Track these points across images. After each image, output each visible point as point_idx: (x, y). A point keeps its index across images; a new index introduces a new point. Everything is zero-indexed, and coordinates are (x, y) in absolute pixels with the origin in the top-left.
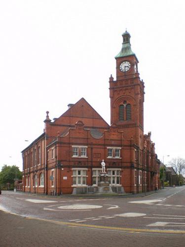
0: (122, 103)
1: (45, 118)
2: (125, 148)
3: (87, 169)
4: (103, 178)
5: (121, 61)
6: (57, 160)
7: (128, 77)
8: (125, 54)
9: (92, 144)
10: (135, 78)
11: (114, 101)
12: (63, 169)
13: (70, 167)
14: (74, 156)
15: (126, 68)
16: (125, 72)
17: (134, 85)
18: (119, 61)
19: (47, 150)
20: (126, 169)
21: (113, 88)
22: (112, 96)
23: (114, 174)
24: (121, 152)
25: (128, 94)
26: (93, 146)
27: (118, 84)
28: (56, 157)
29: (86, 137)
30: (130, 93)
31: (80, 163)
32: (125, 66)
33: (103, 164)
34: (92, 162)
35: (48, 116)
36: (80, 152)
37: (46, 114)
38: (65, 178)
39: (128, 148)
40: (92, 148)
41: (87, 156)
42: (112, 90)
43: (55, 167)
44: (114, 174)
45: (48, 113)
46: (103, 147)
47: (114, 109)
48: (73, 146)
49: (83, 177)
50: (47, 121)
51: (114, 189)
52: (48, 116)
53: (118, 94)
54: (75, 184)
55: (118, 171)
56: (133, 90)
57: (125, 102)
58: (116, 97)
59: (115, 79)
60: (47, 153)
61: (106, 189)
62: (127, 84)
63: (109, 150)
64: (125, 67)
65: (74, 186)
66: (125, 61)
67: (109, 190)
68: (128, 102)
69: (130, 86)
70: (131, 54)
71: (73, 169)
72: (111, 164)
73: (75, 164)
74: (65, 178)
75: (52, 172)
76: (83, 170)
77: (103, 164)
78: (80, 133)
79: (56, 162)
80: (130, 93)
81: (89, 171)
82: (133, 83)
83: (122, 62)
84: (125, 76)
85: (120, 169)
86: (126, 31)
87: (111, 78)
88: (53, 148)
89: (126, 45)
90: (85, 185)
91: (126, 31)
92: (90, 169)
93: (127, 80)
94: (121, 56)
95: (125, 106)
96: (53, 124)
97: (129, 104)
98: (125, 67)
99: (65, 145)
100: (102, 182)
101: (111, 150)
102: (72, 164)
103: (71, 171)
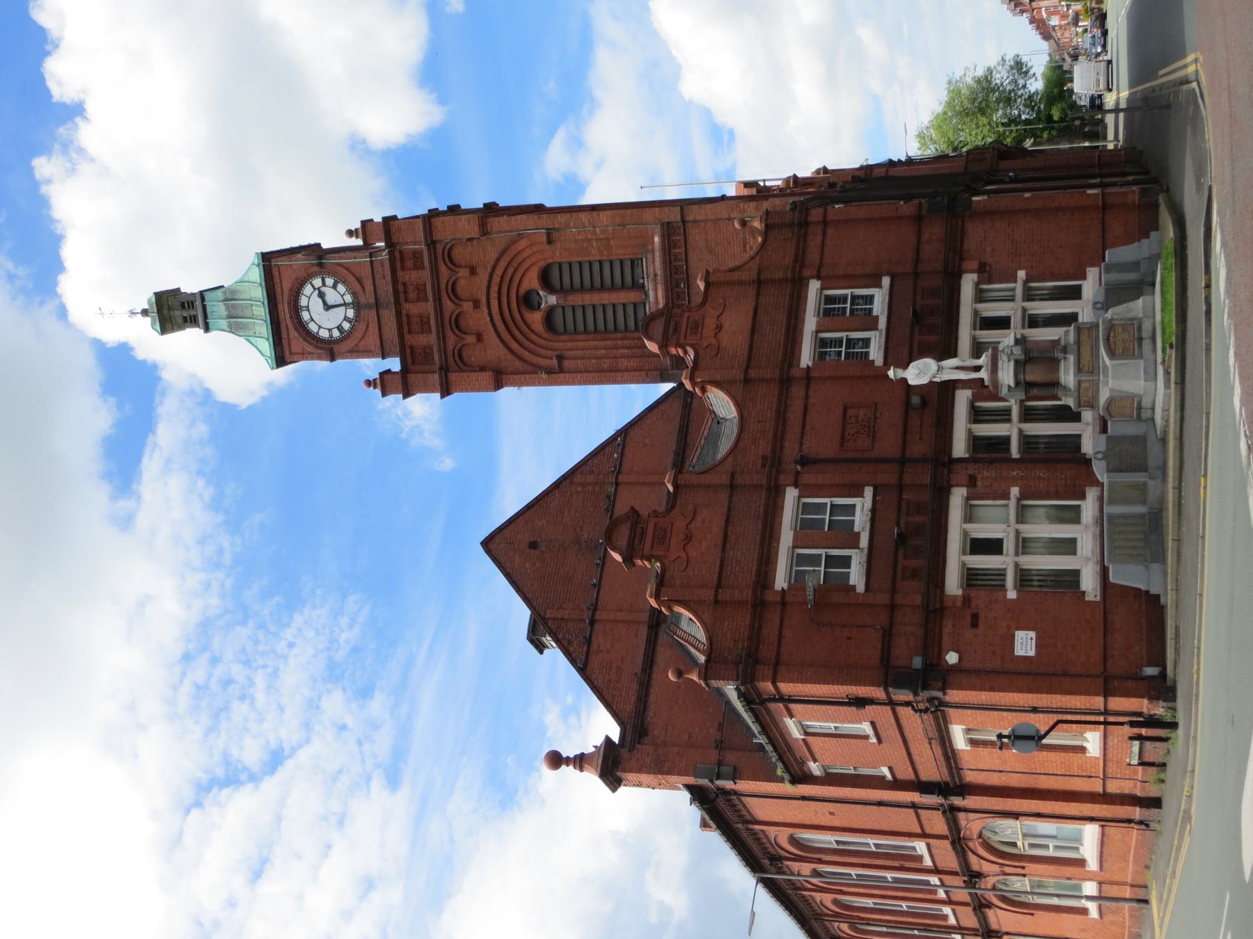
0: (536, 318)
1: (591, 780)
2: (813, 255)
3: (958, 497)
4: (1034, 375)
5: (293, 333)
6: (878, 693)
7: (386, 289)
8: (261, 311)
9: (774, 462)
10: (390, 244)
11: (518, 364)
12: (952, 658)
13: (935, 607)
14: (856, 576)
15: (332, 297)
16: (356, 305)
17: (432, 244)
18: (297, 343)
19: (807, 778)
20: (971, 244)
21: (445, 370)
22: (487, 376)
23: (1002, 323)
24: (850, 280)
26: (791, 449)
27: (420, 340)
28: (860, 702)
29: (723, 497)
30: (473, 271)
31: (912, 540)
32: (326, 308)
33: (920, 372)
34: (903, 461)
35: (580, 761)
36: (822, 537)
37: (568, 771)
38: (1025, 644)
39: (814, 243)
40: (804, 461)
41: (860, 494)
42: (453, 377)
43: (938, 713)
44: (1002, 323)
46: (797, 392)
47: (567, 364)
48: (781, 582)
49: (1020, 519)
50: (612, 765)
51: (1115, 294)
52: (580, 761)
53: (479, 338)
54: (1076, 574)
55: (980, 297)
56: (458, 254)
57: (528, 301)
58: (494, 350)
59: (394, 364)
60: (831, 779)
61: (1127, 342)
62: (421, 289)
63: (820, 357)
64: (328, 307)
65: (1089, 584)
66: (296, 309)
67: (1134, 325)
68: (532, 281)
69: (435, 273)
70: (256, 275)
71: (953, 584)
72: (928, 328)
73: (914, 574)
74: (1025, 644)
75: (973, 742)
76: (969, 517)
77: (920, 372)
78: (688, 538)
79: (892, 703)
81: (972, 482)
82: (417, 255)
83: (302, 327)
84: (377, 305)
85: (968, 283)
86: (145, 312)
87: (384, 383)
88: (793, 729)
89: (217, 308)
90: (1088, 508)
91: (145, 312)
92: (961, 473)
93: (400, 293)
94: (264, 328)
95: (553, 300)
96: (636, 725)
98: (328, 307)
99: (770, 630)
100: (1068, 376)
101: (823, 343)
102: (912, 594)
103: (966, 600)
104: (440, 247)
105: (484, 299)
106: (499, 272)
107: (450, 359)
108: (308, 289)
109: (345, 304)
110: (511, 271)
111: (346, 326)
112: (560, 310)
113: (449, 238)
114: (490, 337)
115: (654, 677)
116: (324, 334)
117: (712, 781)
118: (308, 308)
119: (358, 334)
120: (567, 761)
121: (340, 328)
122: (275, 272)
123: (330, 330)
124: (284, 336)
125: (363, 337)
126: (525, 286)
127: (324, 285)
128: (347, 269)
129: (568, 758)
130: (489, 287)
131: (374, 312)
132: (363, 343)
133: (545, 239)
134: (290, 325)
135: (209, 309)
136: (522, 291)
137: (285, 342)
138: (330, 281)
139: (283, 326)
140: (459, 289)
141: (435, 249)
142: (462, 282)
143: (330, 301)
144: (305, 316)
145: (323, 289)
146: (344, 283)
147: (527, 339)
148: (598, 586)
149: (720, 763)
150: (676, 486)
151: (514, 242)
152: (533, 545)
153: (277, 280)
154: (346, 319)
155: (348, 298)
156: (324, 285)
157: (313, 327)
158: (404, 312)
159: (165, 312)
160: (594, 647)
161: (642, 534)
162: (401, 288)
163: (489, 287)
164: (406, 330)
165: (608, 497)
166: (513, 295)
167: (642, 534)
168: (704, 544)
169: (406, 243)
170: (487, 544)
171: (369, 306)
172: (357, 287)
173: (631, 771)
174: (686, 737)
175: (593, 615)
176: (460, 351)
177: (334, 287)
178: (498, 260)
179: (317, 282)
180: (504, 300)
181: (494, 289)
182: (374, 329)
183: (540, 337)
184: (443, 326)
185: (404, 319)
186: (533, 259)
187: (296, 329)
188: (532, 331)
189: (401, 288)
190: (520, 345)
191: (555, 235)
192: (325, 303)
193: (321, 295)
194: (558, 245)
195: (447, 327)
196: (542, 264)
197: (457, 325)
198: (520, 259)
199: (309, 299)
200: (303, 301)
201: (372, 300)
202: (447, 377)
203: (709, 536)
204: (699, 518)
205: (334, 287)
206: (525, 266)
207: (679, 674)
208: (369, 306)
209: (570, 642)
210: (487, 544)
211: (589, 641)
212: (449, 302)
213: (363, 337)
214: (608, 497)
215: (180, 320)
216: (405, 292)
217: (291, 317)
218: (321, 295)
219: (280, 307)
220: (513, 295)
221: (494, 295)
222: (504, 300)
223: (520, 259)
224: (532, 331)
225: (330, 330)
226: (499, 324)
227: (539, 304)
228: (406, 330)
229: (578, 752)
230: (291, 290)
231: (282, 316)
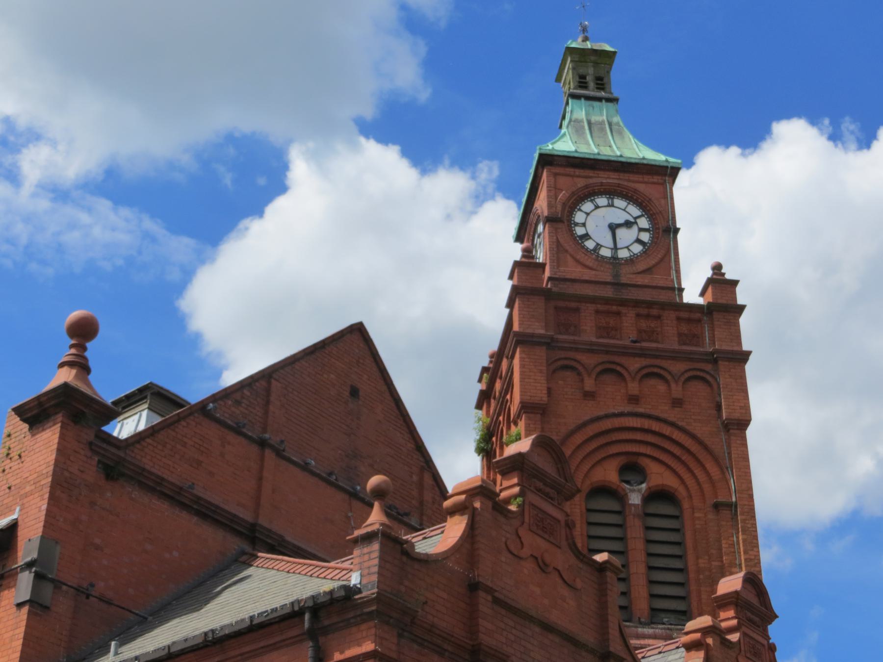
0: (609, 474)
5: (581, 183)
15: (626, 236)
21: (549, 344)
25: (664, 410)
30: (677, 403)
45: (84, 331)
53: (589, 395)
57: (632, 469)
64: (613, 228)
66: (612, 192)
68: (659, 476)
80: (677, 403)
82: (695, 338)
83: (589, 194)
84: (617, 285)
95: (635, 499)
97: (658, 495)
98: (613, 228)
104: (709, 367)
105: (641, 410)
106: (677, 435)
107: (562, 354)
108: (635, 211)
109: (615, 248)
110: (677, 451)
111: (590, 244)
112: (616, 507)
113: (722, 381)
114: (589, 410)
115: (184, 515)
116: (579, 217)
117: (29, 565)
118: (611, 205)
119: (580, 256)
120: (81, 347)
121: (586, 236)
122: (656, 179)
123: (584, 225)
124: (578, 172)
125: (577, 261)
126: (653, 468)
127: (641, 230)
128: (662, 260)
129: (85, 349)
130: (658, 419)
131: (609, 279)
132: (569, 258)
133: (721, 499)
134: (591, 181)
135: (596, 104)
136: (645, 462)
137: (570, 170)
138: (645, 237)
139: (590, 173)
140: (653, 382)
141: (707, 361)
142: (661, 387)
143: (621, 233)
144: (602, 201)
145: (635, 229)
146: (645, 253)
147: (585, 458)
148: (305, 467)
149: (57, 584)
150: (602, 568)
151: (716, 460)
152: (354, 392)
153: (647, 178)
154: (598, 246)
155: (623, 254)
156: (641, 230)
157: (587, 206)
158: (623, 310)
159: (593, 58)
160: (231, 437)
161: (547, 495)
162: (655, 312)
163: (658, 419)
164: (601, 307)
165: (407, 514)
166: (642, 449)
167: (547, 495)
168: (537, 590)
169: (712, 329)
170: (358, 331)
171: (616, 275)
172: (641, 267)
173: (62, 437)
174: (97, 541)
175: (271, 447)
176: (572, 368)
177: (638, 241)
178: (693, 437)
179: (644, 223)
180: (638, 436)
181: (655, 426)
182: (588, 275)
183: (587, 475)
184: (607, 352)
185: (614, 308)
186: (690, 482)
187: (586, 187)
188: (593, 466)
189: (655, 312)
190: (579, 447)
191: (726, 513)
192: (619, 226)
193: (628, 224)
194: (711, 516)
195: (606, 358)
196: (682, 492)
197: (610, 371)
198: (692, 464)
199: (622, 210)
200: (619, 202)
201: (624, 280)
202: (539, 344)
203: (546, 601)
204: (565, 592)
205: (638, 241)
206: (681, 470)
207: (379, 493)
208: (616, 275)
209: (238, 403)
210: (358, 331)
211: (237, 431)
212: (638, 366)
213: (577, 261)
214: (407, 514)
215: (582, 71)
216: (648, 316)
217: (602, 184)
218: (628, 224)
219: (613, 175)
220: (642, 449)
221: (646, 424)
222: (638, 436)
223: (692, 464)
224: (593, 466)
225: (584, 225)
226: (608, 424)
227: (628, 482)
228: (601, 307)
229: (91, 364)
230: (636, 191)
231: (602, 174)
